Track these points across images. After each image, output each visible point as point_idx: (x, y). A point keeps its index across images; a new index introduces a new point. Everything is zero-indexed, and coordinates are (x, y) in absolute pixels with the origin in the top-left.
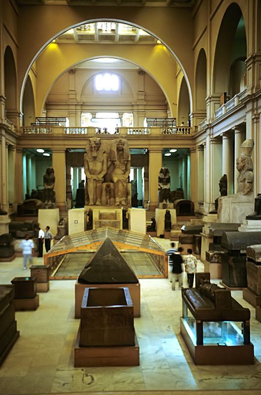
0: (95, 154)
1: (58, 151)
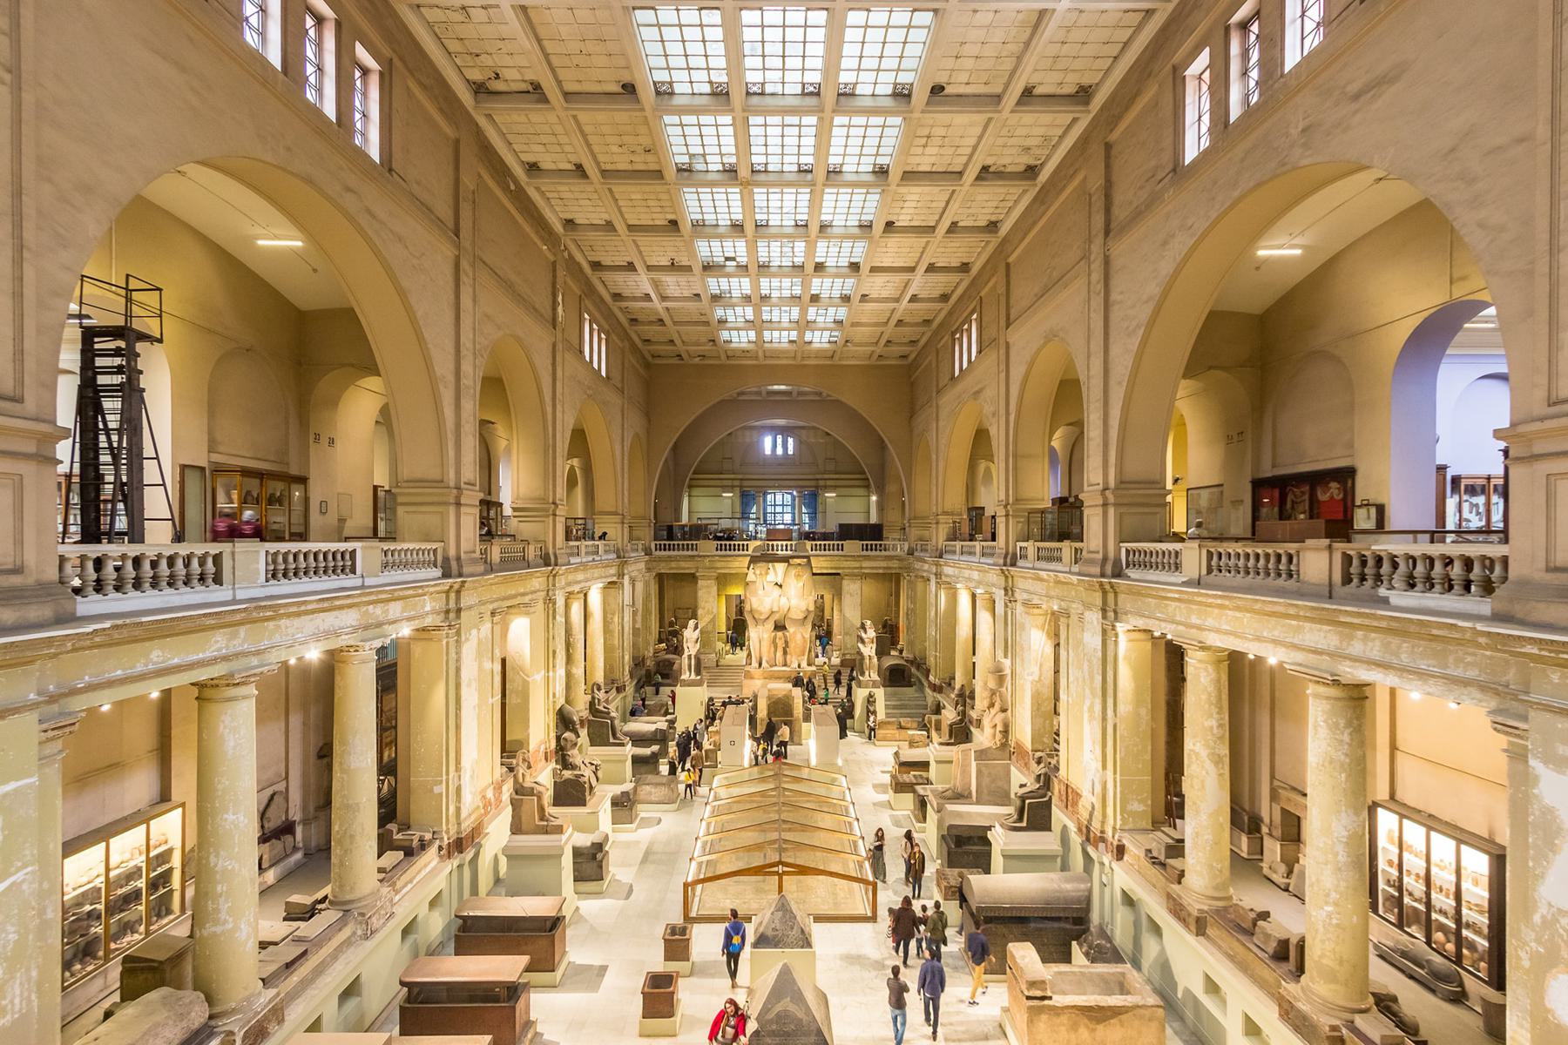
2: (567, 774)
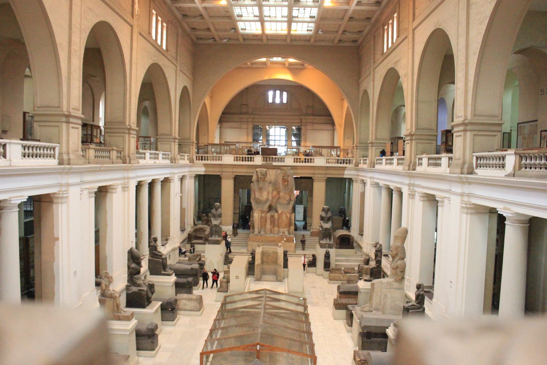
1: (227, 178)
2: (134, 289)
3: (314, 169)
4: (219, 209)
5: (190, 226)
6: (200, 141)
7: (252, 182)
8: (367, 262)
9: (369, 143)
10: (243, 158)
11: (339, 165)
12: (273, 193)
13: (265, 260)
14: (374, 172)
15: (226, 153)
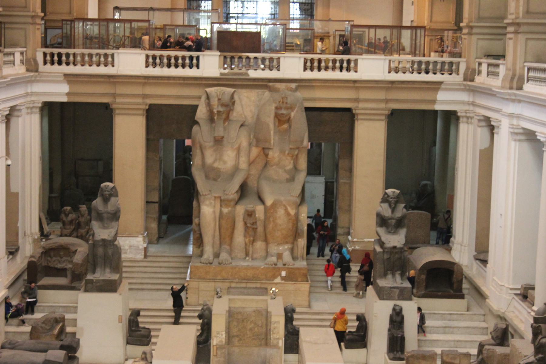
0: (220, 132)
1: (129, 111)
3: (357, 88)
4: (113, 199)
5: (29, 240)
6: (49, 8)
7: (197, 123)
8: (503, 336)
9: (509, 24)
10: (169, 58)
11: (424, 77)
12: (249, 152)
13: (235, 331)
14: (520, 101)
15: (124, 46)
